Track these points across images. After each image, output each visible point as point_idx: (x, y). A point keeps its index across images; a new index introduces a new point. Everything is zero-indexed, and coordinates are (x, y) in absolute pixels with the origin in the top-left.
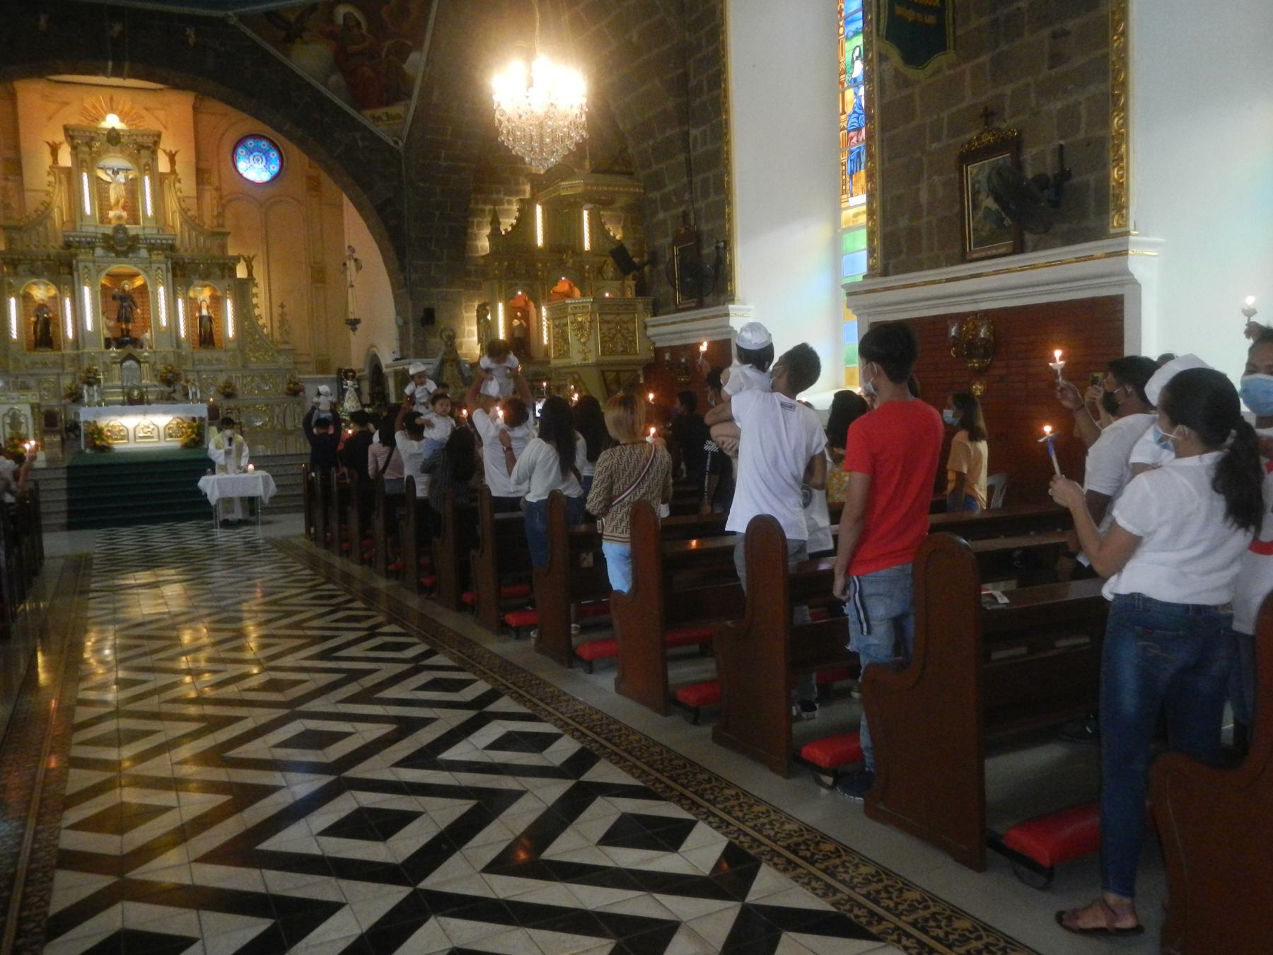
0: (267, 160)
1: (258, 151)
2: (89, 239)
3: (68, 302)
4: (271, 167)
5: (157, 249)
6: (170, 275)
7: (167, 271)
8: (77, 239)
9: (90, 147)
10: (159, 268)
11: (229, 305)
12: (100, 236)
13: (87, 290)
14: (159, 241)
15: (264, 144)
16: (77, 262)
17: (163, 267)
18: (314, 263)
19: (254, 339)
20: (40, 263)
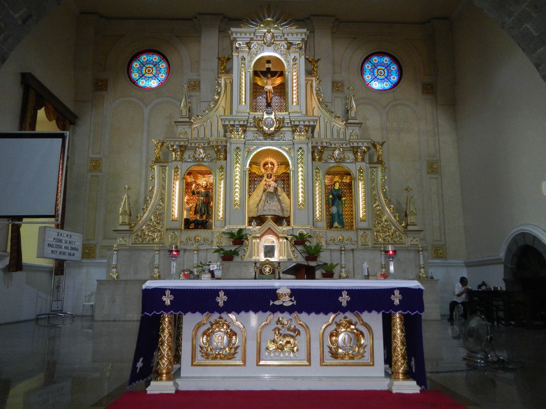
0: (388, 73)
1: (381, 66)
2: (242, 123)
4: (392, 77)
6: (310, 155)
8: (232, 123)
9: (250, 49)
10: (301, 148)
11: (361, 184)
12: (251, 120)
13: (237, 170)
14: (302, 123)
15: (386, 60)
16: (231, 144)
17: (304, 147)
19: (382, 222)
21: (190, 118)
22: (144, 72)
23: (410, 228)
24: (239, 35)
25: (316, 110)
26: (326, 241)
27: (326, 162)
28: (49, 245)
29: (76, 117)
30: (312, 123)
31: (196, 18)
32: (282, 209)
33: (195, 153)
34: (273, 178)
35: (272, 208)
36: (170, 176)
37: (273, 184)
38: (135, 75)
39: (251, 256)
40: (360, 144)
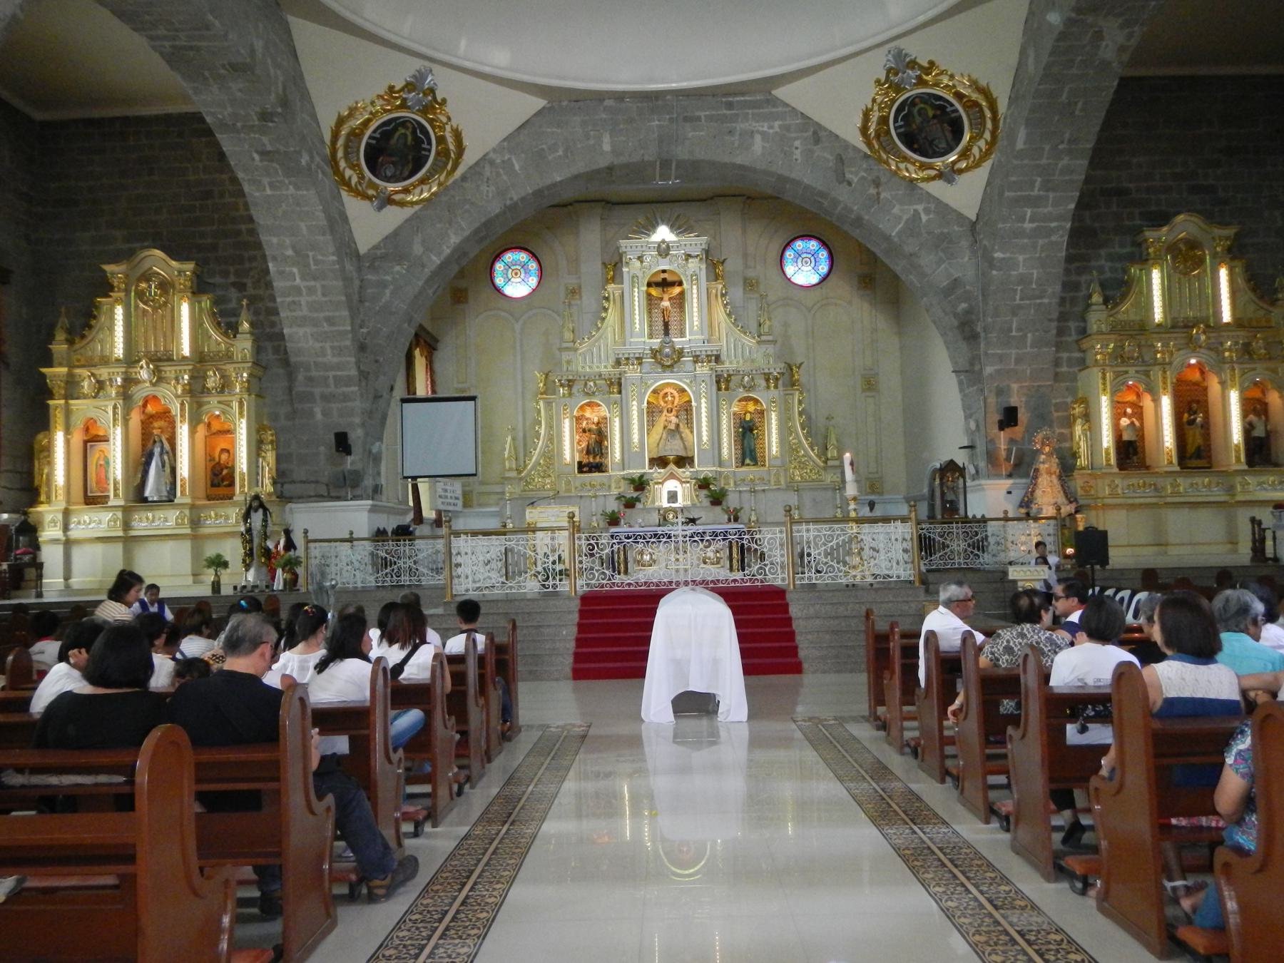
3: (617, 423)
5: (702, 362)
6: (715, 388)
7: (711, 385)
8: (626, 356)
11: (774, 416)
15: (813, 245)
17: (708, 380)
18: (865, 369)
20: (592, 384)
21: (574, 342)
22: (510, 276)
23: (830, 463)
24: (629, 249)
25: (723, 325)
26: (735, 482)
27: (734, 390)
28: (440, 497)
29: (437, 341)
30: (715, 353)
31: (571, 204)
32: (685, 448)
33: (586, 384)
34: (674, 412)
35: (673, 449)
36: (558, 414)
37: (674, 420)
38: (499, 281)
39: (653, 502)
40: (772, 370)
